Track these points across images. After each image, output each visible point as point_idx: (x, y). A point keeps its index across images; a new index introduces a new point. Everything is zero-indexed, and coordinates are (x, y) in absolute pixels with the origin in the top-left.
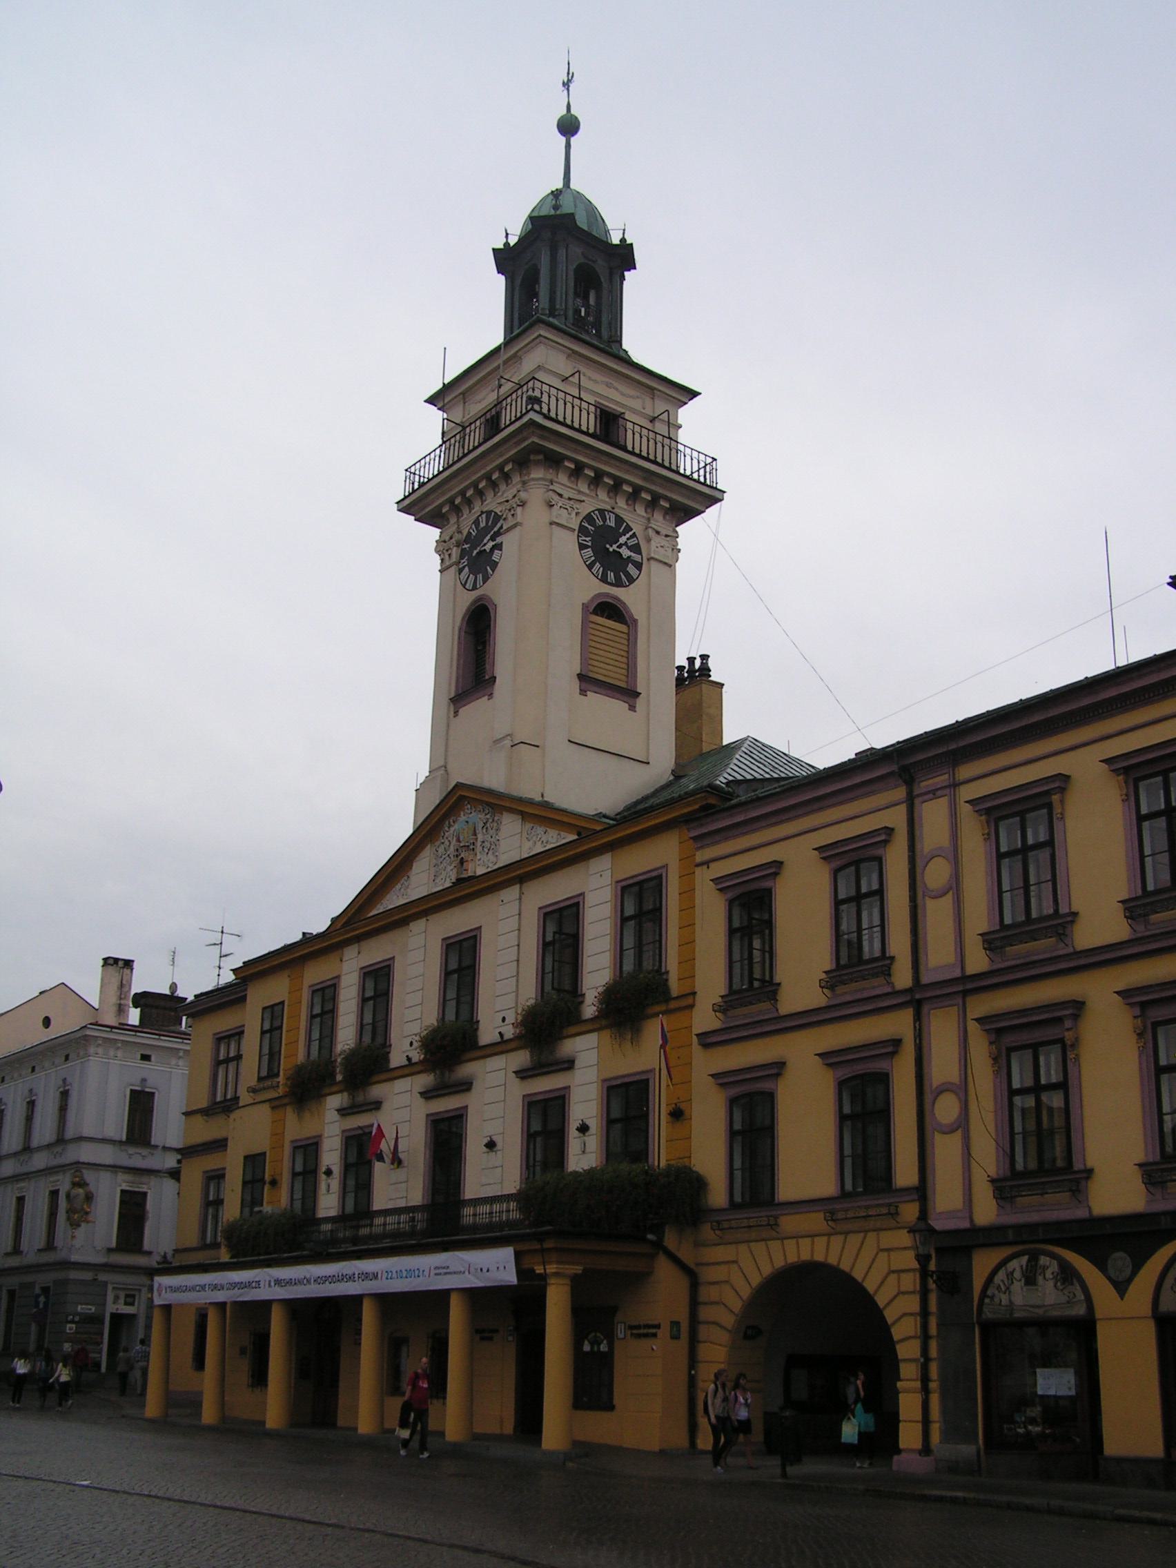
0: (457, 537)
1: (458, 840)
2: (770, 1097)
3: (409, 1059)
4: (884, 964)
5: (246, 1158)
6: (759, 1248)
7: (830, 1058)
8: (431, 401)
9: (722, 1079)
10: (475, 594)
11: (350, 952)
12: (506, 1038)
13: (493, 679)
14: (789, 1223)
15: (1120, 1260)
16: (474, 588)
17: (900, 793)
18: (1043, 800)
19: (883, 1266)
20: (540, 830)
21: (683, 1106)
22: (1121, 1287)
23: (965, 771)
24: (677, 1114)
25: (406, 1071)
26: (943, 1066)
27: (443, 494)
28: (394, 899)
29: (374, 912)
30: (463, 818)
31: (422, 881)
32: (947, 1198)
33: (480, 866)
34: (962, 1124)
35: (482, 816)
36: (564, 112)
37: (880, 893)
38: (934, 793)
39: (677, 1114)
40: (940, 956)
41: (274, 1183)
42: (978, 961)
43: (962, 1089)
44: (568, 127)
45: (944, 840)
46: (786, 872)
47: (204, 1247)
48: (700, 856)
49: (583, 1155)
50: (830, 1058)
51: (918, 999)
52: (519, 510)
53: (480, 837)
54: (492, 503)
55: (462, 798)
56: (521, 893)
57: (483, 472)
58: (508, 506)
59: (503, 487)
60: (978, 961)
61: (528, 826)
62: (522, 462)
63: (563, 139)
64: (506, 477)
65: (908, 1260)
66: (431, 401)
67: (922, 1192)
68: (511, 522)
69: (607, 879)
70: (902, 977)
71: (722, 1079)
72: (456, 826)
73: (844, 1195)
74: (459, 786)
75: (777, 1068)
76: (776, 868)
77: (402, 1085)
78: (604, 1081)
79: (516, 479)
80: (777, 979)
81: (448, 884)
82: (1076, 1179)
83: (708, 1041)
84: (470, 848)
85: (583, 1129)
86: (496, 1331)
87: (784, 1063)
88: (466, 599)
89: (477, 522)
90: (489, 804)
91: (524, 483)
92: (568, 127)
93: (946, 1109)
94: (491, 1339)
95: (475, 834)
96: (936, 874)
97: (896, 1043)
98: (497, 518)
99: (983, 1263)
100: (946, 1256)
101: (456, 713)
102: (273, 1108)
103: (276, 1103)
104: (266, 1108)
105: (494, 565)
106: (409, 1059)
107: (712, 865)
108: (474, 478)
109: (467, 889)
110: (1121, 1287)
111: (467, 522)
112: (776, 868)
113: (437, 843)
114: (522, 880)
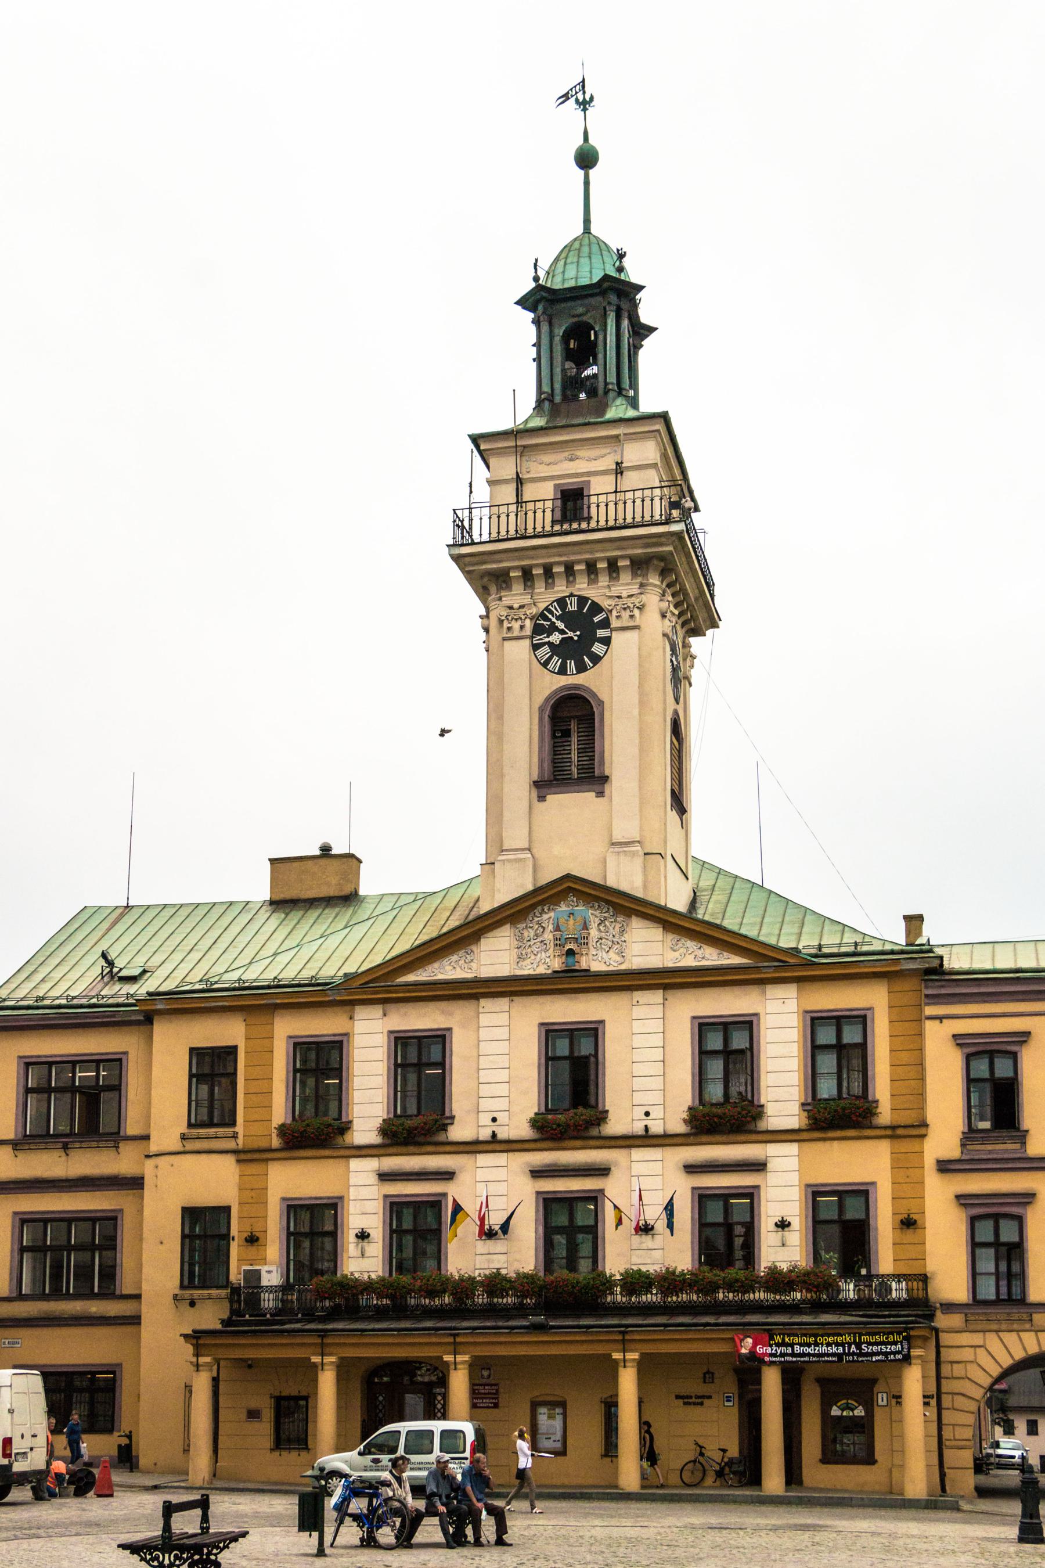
0: (534, 611)
1: (557, 928)
3: (494, 1135)
5: (184, 1210)
10: (563, 681)
11: (361, 1012)
12: (650, 1133)
13: (605, 779)
16: (562, 671)
20: (690, 944)
21: (914, 1217)
24: (908, 1223)
25: (490, 1147)
27: (520, 559)
29: (411, 978)
30: (563, 908)
31: (496, 956)
35: (597, 913)
36: (581, 141)
39: (908, 1223)
41: (252, 1240)
46: (1033, 1042)
49: (783, 1249)
52: (636, 612)
53: (594, 933)
54: (599, 592)
55: (570, 888)
56: (665, 999)
57: (588, 556)
58: (620, 602)
59: (604, 580)
61: (671, 938)
62: (639, 565)
63: (582, 172)
64: (613, 568)
68: (625, 621)
69: (792, 1005)
72: (552, 914)
74: (568, 877)
77: (483, 1159)
78: (808, 1186)
79: (625, 577)
81: (542, 970)
84: (583, 941)
85: (783, 1225)
86: (710, 1397)
87: (1033, 1195)
88: (552, 683)
89: (562, 602)
90: (608, 902)
91: (642, 585)
94: (702, 1404)
95: (585, 927)
98: (596, 608)
101: (542, 798)
102: (238, 1161)
103: (243, 1157)
104: (230, 1160)
105: (596, 659)
106: (494, 1135)
107: (944, 1021)
108: (573, 558)
109: (571, 980)
111: (545, 597)
113: (521, 926)
114: (666, 987)
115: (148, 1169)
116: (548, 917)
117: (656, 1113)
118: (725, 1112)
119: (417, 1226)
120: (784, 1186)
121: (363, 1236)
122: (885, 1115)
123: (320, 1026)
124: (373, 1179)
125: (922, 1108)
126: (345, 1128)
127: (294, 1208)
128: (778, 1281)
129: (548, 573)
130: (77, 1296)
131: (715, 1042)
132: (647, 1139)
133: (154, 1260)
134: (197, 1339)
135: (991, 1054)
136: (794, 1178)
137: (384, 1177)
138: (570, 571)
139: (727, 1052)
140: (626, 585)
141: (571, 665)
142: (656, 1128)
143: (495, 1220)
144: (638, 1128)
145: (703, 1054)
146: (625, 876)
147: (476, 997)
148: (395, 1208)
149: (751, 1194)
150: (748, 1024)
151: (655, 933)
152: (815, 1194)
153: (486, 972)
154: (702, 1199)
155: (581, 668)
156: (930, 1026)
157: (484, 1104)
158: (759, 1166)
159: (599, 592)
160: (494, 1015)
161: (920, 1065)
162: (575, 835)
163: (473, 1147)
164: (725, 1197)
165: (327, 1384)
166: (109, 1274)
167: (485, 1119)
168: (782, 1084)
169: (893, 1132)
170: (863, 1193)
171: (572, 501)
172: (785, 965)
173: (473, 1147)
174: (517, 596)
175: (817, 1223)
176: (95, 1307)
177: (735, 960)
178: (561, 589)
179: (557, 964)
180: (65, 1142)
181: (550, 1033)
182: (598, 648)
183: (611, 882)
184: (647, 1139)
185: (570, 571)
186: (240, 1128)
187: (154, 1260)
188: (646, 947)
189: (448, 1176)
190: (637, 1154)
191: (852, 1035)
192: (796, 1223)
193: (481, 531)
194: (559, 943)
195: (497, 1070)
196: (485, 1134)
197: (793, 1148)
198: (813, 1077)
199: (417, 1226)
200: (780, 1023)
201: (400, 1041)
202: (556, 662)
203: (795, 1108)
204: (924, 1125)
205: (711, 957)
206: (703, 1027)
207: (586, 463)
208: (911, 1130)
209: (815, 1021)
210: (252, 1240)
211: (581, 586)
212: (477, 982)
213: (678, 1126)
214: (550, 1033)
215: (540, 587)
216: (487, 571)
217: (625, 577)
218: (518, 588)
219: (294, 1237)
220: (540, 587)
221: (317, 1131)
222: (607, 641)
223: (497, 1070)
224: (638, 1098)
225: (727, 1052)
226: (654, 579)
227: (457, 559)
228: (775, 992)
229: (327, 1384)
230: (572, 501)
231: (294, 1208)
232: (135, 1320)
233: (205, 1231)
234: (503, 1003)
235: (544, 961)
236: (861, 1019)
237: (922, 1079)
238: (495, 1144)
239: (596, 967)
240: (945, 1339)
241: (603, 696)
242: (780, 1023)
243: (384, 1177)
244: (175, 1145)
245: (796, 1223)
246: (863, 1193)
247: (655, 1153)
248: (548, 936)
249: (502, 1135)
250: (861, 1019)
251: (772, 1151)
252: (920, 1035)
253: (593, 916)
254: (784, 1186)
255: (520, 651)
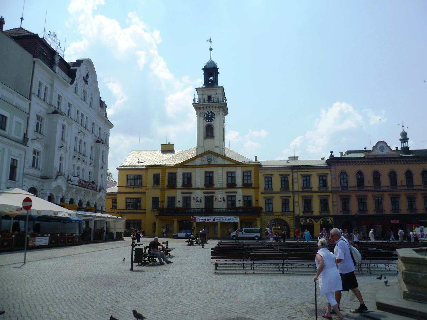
2: (272, 200)
4: (288, 188)
6: (271, 217)
7: (281, 197)
8: (196, 89)
9: (264, 197)
10: (208, 123)
11: (179, 169)
14: (275, 214)
15: (317, 220)
16: (208, 121)
17: (291, 171)
18: (309, 176)
19: (289, 219)
20: (226, 161)
22: (317, 222)
23: (299, 170)
24: (257, 201)
26: (296, 199)
28: (192, 163)
29: (186, 164)
30: (208, 155)
31: (198, 162)
32: (297, 213)
33: (213, 163)
34: (298, 206)
37: (288, 181)
38: (296, 172)
39: (257, 201)
40: (296, 189)
41: (163, 202)
42: (300, 190)
43: (298, 202)
44: (211, 49)
45: (297, 177)
47: (127, 209)
48: (260, 171)
49: (239, 204)
50: (281, 197)
51: (293, 192)
53: (212, 159)
60: (300, 190)
62: (219, 107)
65: (293, 219)
66: (196, 89)
67: (294, 212)
69: (241, 170)
70: (291, 190)
71: (264, 197)
73: (283, 211)
75: (273, 197)
76: (272, 175)
79: (217, 109)
80: (273, 187)
82: (312, 212)
83: (262, 193)
84: (211, 160)
85: (239, 201)
89: (208, 112)
92: (211, 49)
93: (297, 204)
96: (296, 180)
97: (290, 197)
98: (213, 113)
99: (301, 219)
100: (297, 218)
101: (205, 139)
104: (159, 190)
105: (213, 120)
109: (209, 165)
110: (317, 222)
111: (206, 111)
112: (272, 175)
114: (223, 167)
115: (147, 191)
116: (206, 156)
117: (221, 185)
118: (231, 185)
119: (187, 200)
120: (239, 195)
121: (179, 201)
122: (253, 185)
123: (172, 171)
124: (180, 193)
125: (259, 185)
126: (176, 186)
127: (169, 198)
128: (239, 208)
129: (206, 108)
130: (139, 209)
131: (230, 175)
132: (220, 188)
133: (147, 204)
134: (156, 216)
135: (268, 177)
136: (241, 194)
137: (182, 193)
138: (209, 107)
139: (232, 176)
140: (217, 110)
141: (209, 121)
142: (221, 187)
143: (199, 200)
144: (219, 187)
145: (228, 177)
146: (217, 151)
147: (195, 167)
148: (184, 198)
149: (235, 197)
150: (234, 172)
151: (222, 159)
152: (244, 197)
153: (197, 164)
154: (228, 197)
155: (211, 121)
156: (260, 174)
157: (197, 183)
158: (236, 192)
159: (213, 111)
160: (198, 170)
161: (258, 178)
162: (210, 144)
163: (195, 189)
164: (231, 197)
165: (176, 223)
166: (140, 206)
167: (197, 185)
168: (239, 181)
169: (255, 188)
170: (251, 196)
171: (210, 98)
172: (240, 164)
173: (195, 189)
174: (202, 111)
175: (244, 201)
176: (138, 211)
177: (233, 163)
178: (208, 110)
179: (207, 163)
180: (134, 187)
181: (206, 173)
182: (213, 119)
183: (215, 152)
184: (220, 188)
185: (209, 107)
186: (160, 185)
187: (147, 204)
188: (220, 161)
189: (191, 193)
190: (219, 190)
191: (249, 174)
192: (241, 201)
193: (196, 102)
194: (207, 160)
195: (198, 178)
196: (197, 187)
197: (241, 190)
198: (243, 180)
199: (187, 200)
200: (239, 172)
201: (184, 173)
202: (207, 120)
203: (241, 184)
204: (259, 187)
205: (229, 163)
206: (228, 173)
207: (211, 92)
208: (257, 187)
209: (244, 172)
210: (163, 202)
211: (211, 110)
212: (196, 165)
213: (225, 186)
214: (206, 173)
215: (205, 109)
216: (197, 107)
217: (217, 109)
218: (202, 109)
219: (168, 201)
220: (205, 109)
221: (172, 185)
222: (214, 118)
223: (198, 178)
224: (219, 183)
225: (232, 176)
226: (221, 109)
227: (193, 105)
228: (238, 168)
229: (176, 223)
230: (210, 98)
231: (169, 198)
232: (145, 213)
233: (155, 201)
234: (199, 168)
235: (205, 163)
236: (250, 172)
237: (259, 181)
238: (198, 189)
239: (213, 164)
240: (262, 217)
241: (214, 125)
242: (239, 172)
243: (182, 193)
244: (151, 187)
245: (241, 201)
246: (251, 196)
247: (221, 190)
248: (206, 159)
249: (199, 187)
250: (250, 172)
251: (238, 190)
252: (258, 175)
253: (213, 156)
254: (239, 195)
255: (202, 118)
